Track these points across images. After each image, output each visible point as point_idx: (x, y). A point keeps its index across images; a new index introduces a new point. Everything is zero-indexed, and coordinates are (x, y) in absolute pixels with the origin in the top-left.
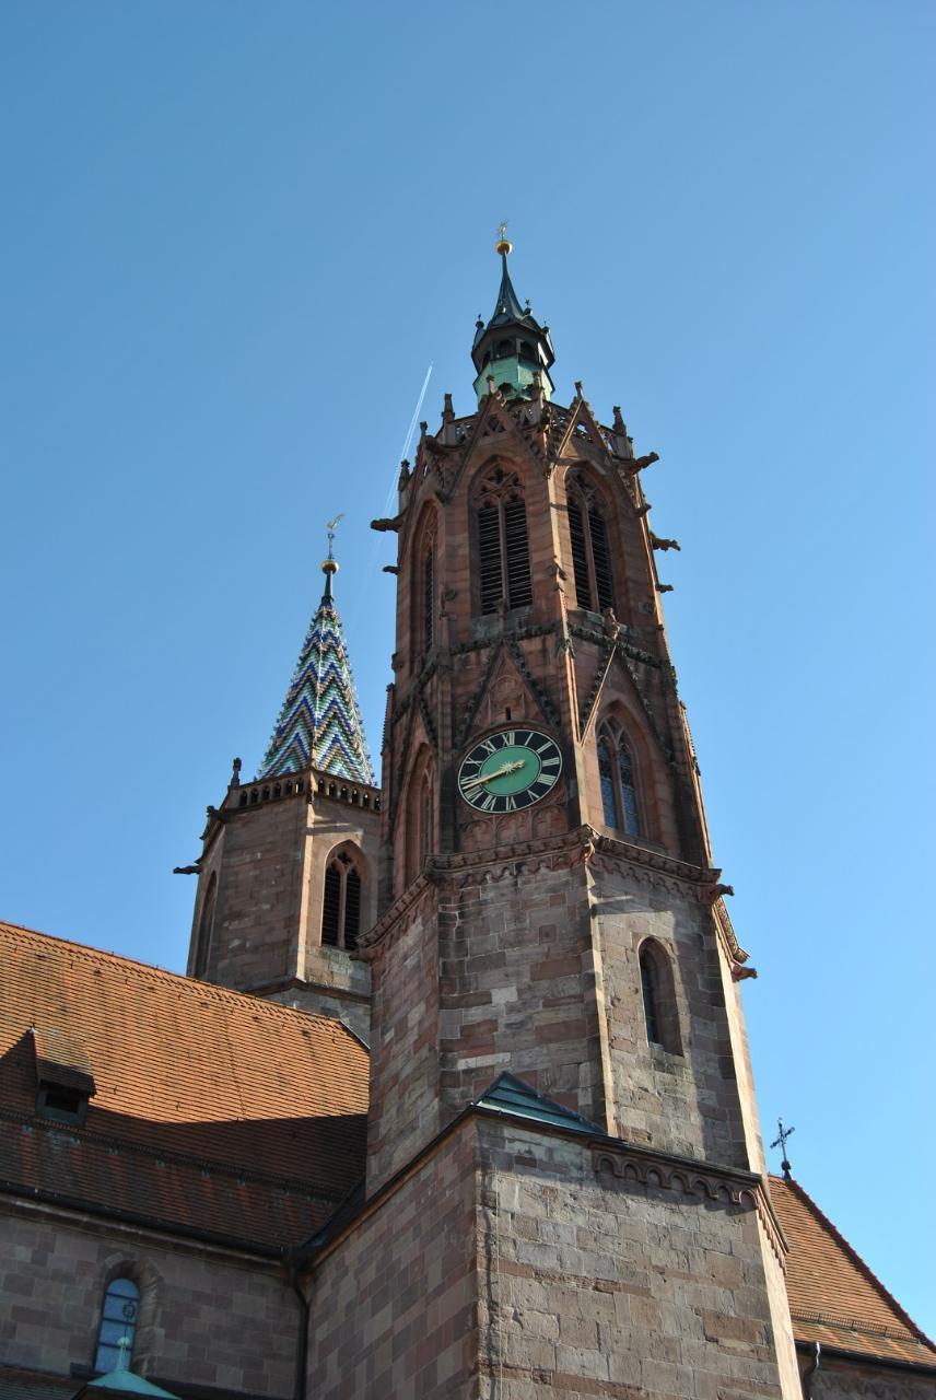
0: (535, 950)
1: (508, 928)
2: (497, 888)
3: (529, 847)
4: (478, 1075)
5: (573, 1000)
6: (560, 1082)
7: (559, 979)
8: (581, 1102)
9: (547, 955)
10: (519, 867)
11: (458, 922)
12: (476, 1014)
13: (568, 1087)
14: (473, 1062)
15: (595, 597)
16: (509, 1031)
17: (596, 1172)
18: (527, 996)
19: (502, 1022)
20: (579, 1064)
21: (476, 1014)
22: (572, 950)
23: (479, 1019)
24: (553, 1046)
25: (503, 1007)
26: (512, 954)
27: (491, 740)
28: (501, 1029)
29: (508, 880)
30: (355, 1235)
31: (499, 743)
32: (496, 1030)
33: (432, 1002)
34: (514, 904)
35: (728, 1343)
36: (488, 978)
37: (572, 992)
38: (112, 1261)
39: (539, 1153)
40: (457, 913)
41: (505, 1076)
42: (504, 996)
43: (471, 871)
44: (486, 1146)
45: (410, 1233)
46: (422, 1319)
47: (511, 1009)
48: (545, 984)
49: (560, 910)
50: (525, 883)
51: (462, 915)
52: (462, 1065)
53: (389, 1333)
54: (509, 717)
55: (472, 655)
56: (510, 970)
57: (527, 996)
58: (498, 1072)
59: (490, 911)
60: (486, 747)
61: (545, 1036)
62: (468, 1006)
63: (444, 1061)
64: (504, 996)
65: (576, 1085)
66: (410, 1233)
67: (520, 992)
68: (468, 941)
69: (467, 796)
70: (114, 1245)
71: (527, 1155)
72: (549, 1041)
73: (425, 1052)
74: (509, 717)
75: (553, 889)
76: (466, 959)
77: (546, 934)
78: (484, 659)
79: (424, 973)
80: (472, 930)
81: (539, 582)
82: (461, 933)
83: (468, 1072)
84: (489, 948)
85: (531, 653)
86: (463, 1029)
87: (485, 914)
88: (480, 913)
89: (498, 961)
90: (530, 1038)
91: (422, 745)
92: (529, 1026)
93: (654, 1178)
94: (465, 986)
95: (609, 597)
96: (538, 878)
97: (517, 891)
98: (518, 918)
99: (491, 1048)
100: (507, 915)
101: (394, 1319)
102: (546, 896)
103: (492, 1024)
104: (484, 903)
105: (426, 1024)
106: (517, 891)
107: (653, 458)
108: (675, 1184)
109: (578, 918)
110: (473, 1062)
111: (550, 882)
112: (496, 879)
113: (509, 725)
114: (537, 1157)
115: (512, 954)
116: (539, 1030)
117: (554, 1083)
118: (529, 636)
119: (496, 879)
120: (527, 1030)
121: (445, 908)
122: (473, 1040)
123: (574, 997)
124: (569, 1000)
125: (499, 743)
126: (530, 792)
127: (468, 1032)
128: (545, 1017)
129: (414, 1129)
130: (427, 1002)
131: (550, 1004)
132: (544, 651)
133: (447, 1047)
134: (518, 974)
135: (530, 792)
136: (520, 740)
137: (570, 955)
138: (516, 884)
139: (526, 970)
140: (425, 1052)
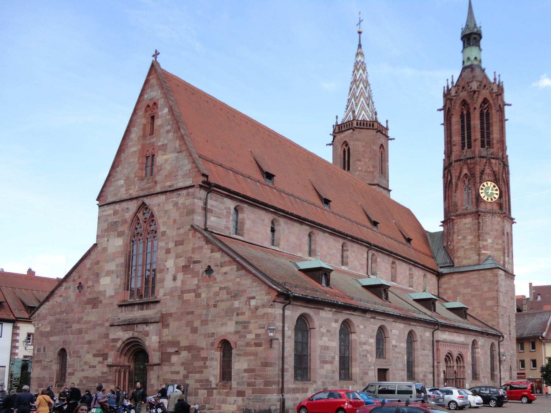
1: (490, 227)
10: (493, 215)
11: (482, 224)
12: (485, 243)
18: (493, 242)
19: (489, 245)
21: (485, 243)
24: (497, 252)
26: (491, 233)
29: (490, 218)
32: (488, 247)
34: (491, 223)
36: (487, 237)
40: (482, 222)
41: (490, 256)
47: (491, 243)
48: (496, 240)
52: (483, 252)
55: (482, 159)
57: (493, 242)
58: (488, 255)
59: (487, 223)
61: (496, 250)
62: (484, 241)
63: (480, 251)
64: (490, 241)
65: (500, 260)
67: (492, 241)
68: (484, 228)
77: (497, 230)
82: (482, 226)
83: (484, 253)
86: (483, 245)
89: (488, 234)
94: (483, 237)
97: (492, 220)
99: (487, 250)
100: (490, 225)
103: (487, 245)
104: (486, 221)
106: (492, 220)
112: (488, 217)
115: (491, 233)
117: (497, 259)
118: (494, 158)
119: (488, 217)
122: (485, 248)
127: (484, 246)
132: (496, 163)
138: (492, 219)
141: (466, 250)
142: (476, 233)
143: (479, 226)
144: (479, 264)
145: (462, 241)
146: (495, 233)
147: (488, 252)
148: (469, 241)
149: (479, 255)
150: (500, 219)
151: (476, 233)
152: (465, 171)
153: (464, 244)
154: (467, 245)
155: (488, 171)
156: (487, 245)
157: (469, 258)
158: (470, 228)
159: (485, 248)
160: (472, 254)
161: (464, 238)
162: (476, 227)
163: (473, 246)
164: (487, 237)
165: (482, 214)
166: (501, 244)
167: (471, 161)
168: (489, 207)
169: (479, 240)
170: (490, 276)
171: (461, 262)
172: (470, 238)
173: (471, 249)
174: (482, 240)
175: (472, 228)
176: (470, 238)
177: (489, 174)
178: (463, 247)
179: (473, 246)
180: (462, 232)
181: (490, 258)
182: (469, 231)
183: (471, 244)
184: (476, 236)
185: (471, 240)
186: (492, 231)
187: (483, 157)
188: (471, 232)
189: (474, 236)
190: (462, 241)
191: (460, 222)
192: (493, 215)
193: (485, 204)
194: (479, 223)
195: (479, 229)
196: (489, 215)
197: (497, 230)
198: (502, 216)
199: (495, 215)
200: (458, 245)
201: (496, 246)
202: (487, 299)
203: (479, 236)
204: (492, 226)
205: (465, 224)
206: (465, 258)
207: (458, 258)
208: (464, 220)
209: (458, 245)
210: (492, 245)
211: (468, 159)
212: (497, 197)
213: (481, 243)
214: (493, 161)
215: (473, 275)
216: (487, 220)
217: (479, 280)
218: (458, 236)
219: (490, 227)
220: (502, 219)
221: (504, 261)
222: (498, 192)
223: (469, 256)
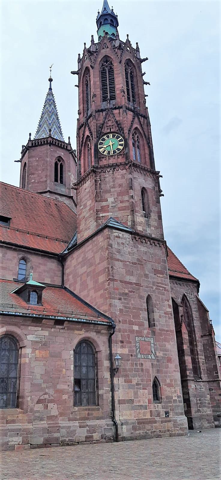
0: (118, 189)
1: (112, 184)
2: (109, 174)
3: (116, 164)
4: (105, 217)
5: (127, 201)
6: (124, 220)
7: (123, 196)
8: (128, 224)
9: (121, 191)
10: (114, 169)
12: (104, 204)
13: (126, 221)
14: (104, 215)
15: (131, 99)
16: (112, 208)
17: (132, 240)
18: (116, 200)
20: (128, 216)
21: (104, 204)
22: (127, 190)
23: (105, 205)
25: (110, 202)
27: (106, 136)
28: (110, 207)
29: (111, 172)
30: (76, 251)
31: (108, 137)
33: (93, 200)
35: (159, 275)
36: (107, 196)
37: (126, 200)
38: (20, 256)
39: (121, 235)
40: (99, 180)
43: (102, 170)
44: (110, 234)
45: (91, 251)
46: (95, 269)
47: (112, 203)
49: (124, 180)
50: (115, 173)
51: (100, 180)
52: (101, 215)
53: (86, 272)
54: (110, 130)
55: (101, 113)
56: (112, 194)
59: (107, 179)
60: (105, 138)
61: (120, 209)
64: (111, 200)
66: (91, 251)
69: (101, 150)
70: (21, 253)
71: (118, 236)
72: (121, 210)
73: (92, 212)
74: (110, 130)
75: (122, 175)
76: (102, 191)
77: (120, 186)
78: (104, 114)
79: (91, 193)
80: (103, 184)
81: (118, 94)
82: (100, 184)
84: (107, 188)
85: (116, 113)
87: (106, 180)
88: (105, 180)
89: (109, 192)
90: (117, 209)
91: (88, 136)
92: (117, 207)
93: (144, 241)
95: (134, 98)
96: (119, 172)
98: (114, 181)
100: (111, 180)
101: (87, 269)
102: (120, 177)
103: (108, 206)
105: (92, 205)
107: (147, 59)
108: (149, 242)
109: (128, 182)
110: (104, 215)
111: (121, 173)
113: (110, 133)
114: (120, 236)
115: (112, 190)
118: (115, 108)
120: (116, 208)
121: (96, 178)
122: (104, 209)
123: (127, 201)
124: (126, 201)
125: (108, 137)
126: (116, 150)
128: (121, 205)
129: (89, 229)
130: (92, 200)
131: (121, 202)
132: (119, 113)
133: (97, 211)
134: (114, 195)
135: (116, 150)
136: (113, 136)
137: (126, 191)
139: (116, 194)
140: (92, 212)
147: (110, 214)
150: (124, 171)
156: (108, 206)
164: (107, 196)
165: (100, 171)
166: (128, 201)
168: (112, 161)
177: (110, 126)
186: (114, 187)
187: (102, 111)
192: (114, 169)
196: (109, 170)
198: (127, 167)
199: (117, 168)
202: (99, 274)
204: (114, 181)
210: (114, 205)
214: (116, 112)
221: (133, 221)
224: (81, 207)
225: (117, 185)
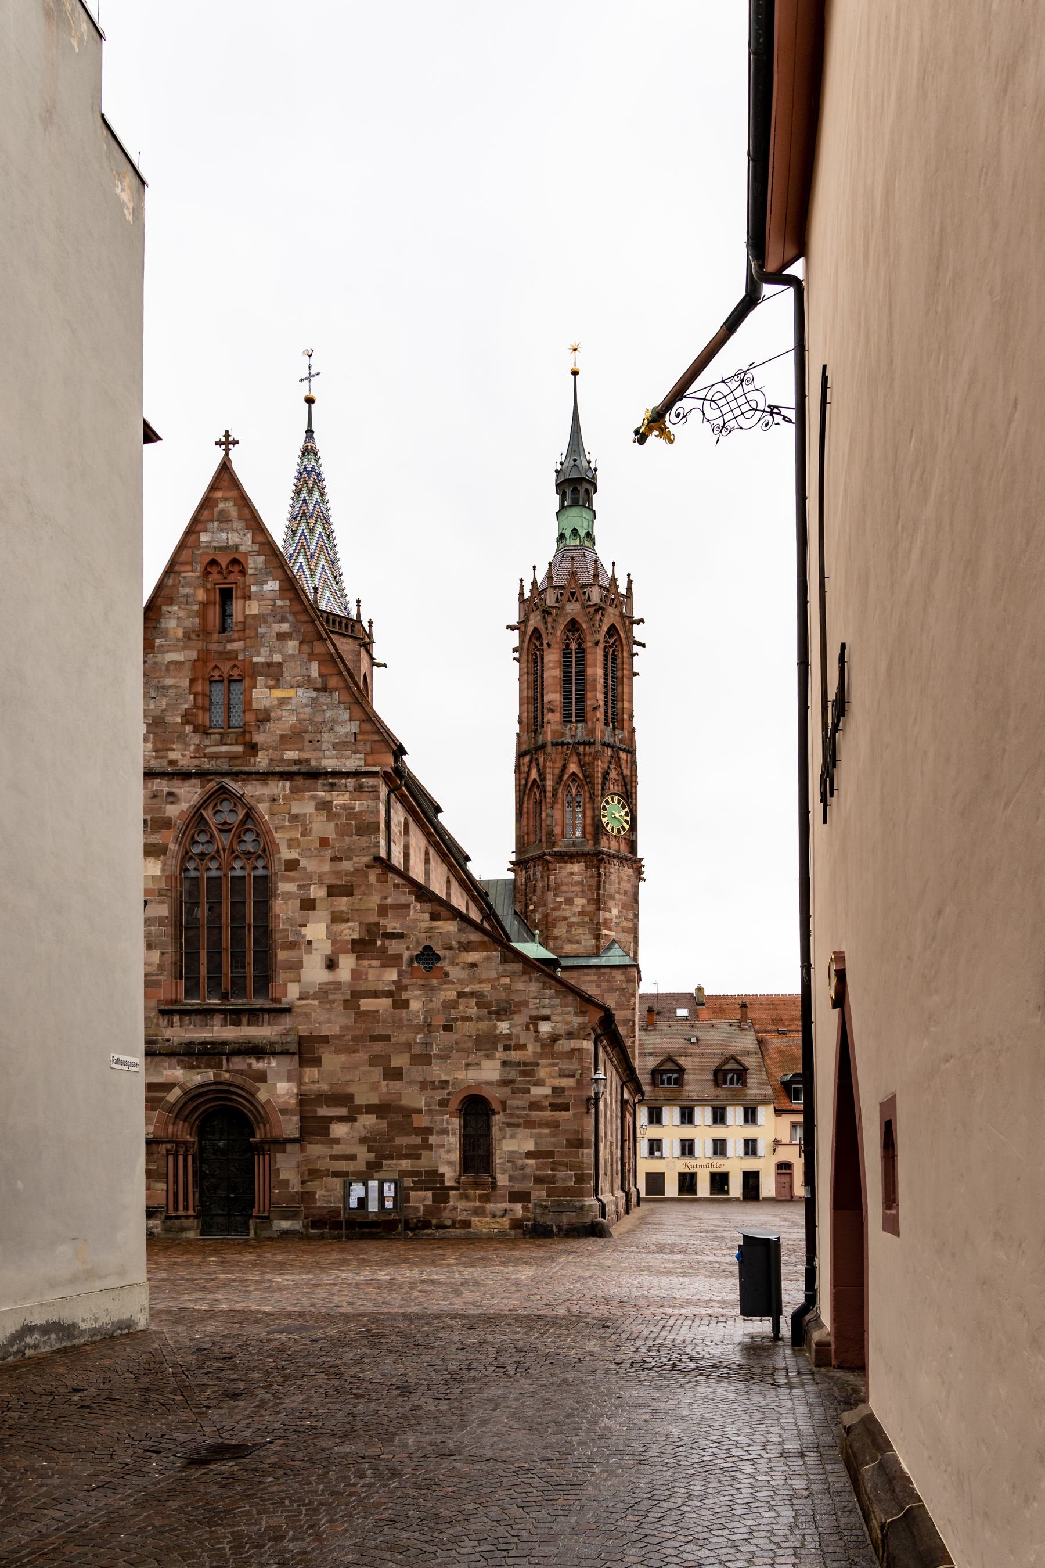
12: (607, 915)
19: (614, 920)
21: (607, 915)
26: (617, 896)
29: (617, 867)
42: (615, 911)
52: (604, 932)
64: (615, 911)
75: (628, 876)
77: (626, 893)
89: (613, 898)
98: (619, 883)
99: (610, 929)
104: (610, 873)
115: (617, 896)
116: (622, 927)
131: (626, 919)
141: (571, 925)
142: (593, 893)
143: (599, 882)
144: (597, 955)
145: (563, 906)
146: (622, 897)
148: (579, 909)
149: (598, 937)
150: (631, 870)
151: (593, 893)
152: (573, 768)
153: (568, 914)
154: (574, 915)
155: (613, 774)
157: (578, 942)
158: (582, 882)
159: (607, 924)
160: (584, 934)
161: (569, 901)
162: (593, 882)
163: (587, 919)
164: (611, 903)
167: (585, 749)
169: (599, 909)
170: (620, 981)
171: (562, 948)
172: (580, 902)
173: (581, 924)
174: (605, 910)
175: (585, 883)
176: (580, 902)
178: (565, 919)
179: (587, 919)
180: (564, 888)
181: (617, 946)
182: (578, 889)
183: (582, 913)
184: (593, 900)
185: (583, 906)
186: (619, 893)
188: (583, 891)
189: (589, 901)
190: (563, 906)
191: (561, 868)
193: (608, 839)
194: (599, 874)
195: (599, 889)
196: (615, 861)
197: (626, 893)
199: (624, 863)
200: (556, 913)
201: (624, 924)
203: (598, 901)
204: (619, 883)
205: (572, 874)
206: (570, 941)
207: (556, 938)
208: (569, 865)
209: (556, 913)
210: (618, 921)
211: (579, 743)
212: (627, 827)
213: (603, 915)
215: (587, 974)
216: (612, 871)
217: (598, 986)
218: (556, 895)
219: (617, 886)
220: (634, 872)
222: (628, 818)
223: (577, 938)
224: (559, 899)
225: (622, 891)
